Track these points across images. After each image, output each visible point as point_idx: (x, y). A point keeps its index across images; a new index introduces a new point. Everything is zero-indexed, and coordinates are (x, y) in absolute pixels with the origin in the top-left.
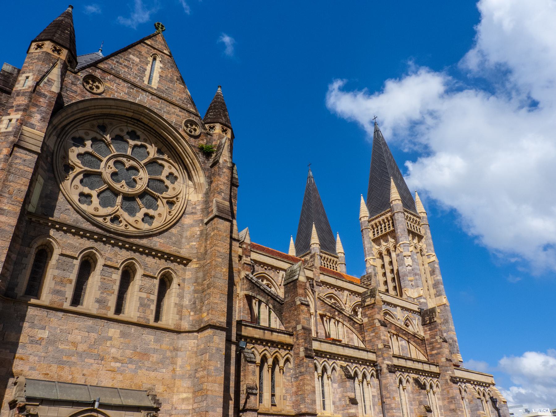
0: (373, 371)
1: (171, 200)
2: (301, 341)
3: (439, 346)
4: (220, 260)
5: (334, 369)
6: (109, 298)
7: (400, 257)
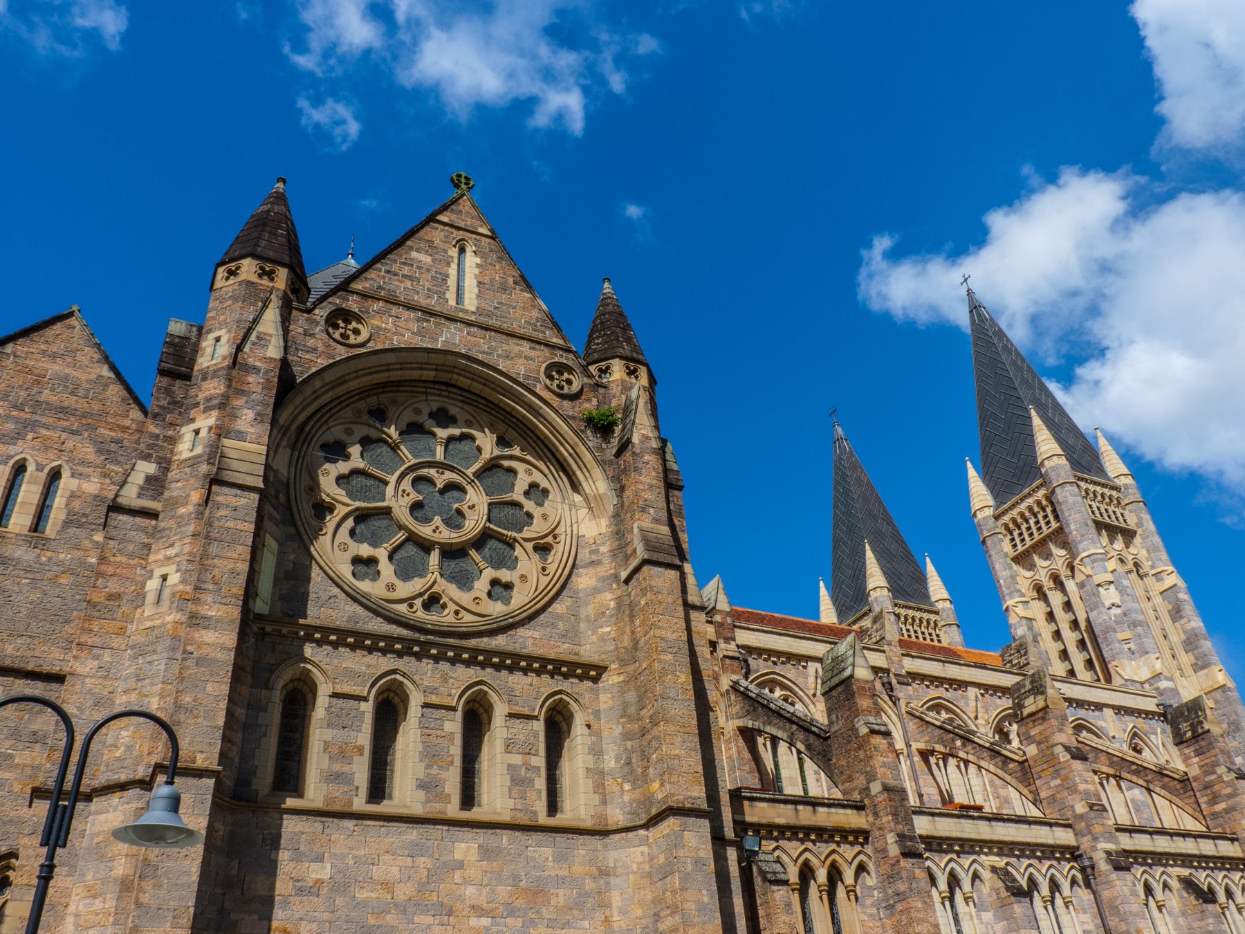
0: (1073, 872)
1: (542, 541)
2: (886, 819)
3: (1229, 790)
4: (670, 657)
5: (976, 876)
6: (444, 775)
7: (1088, 588)
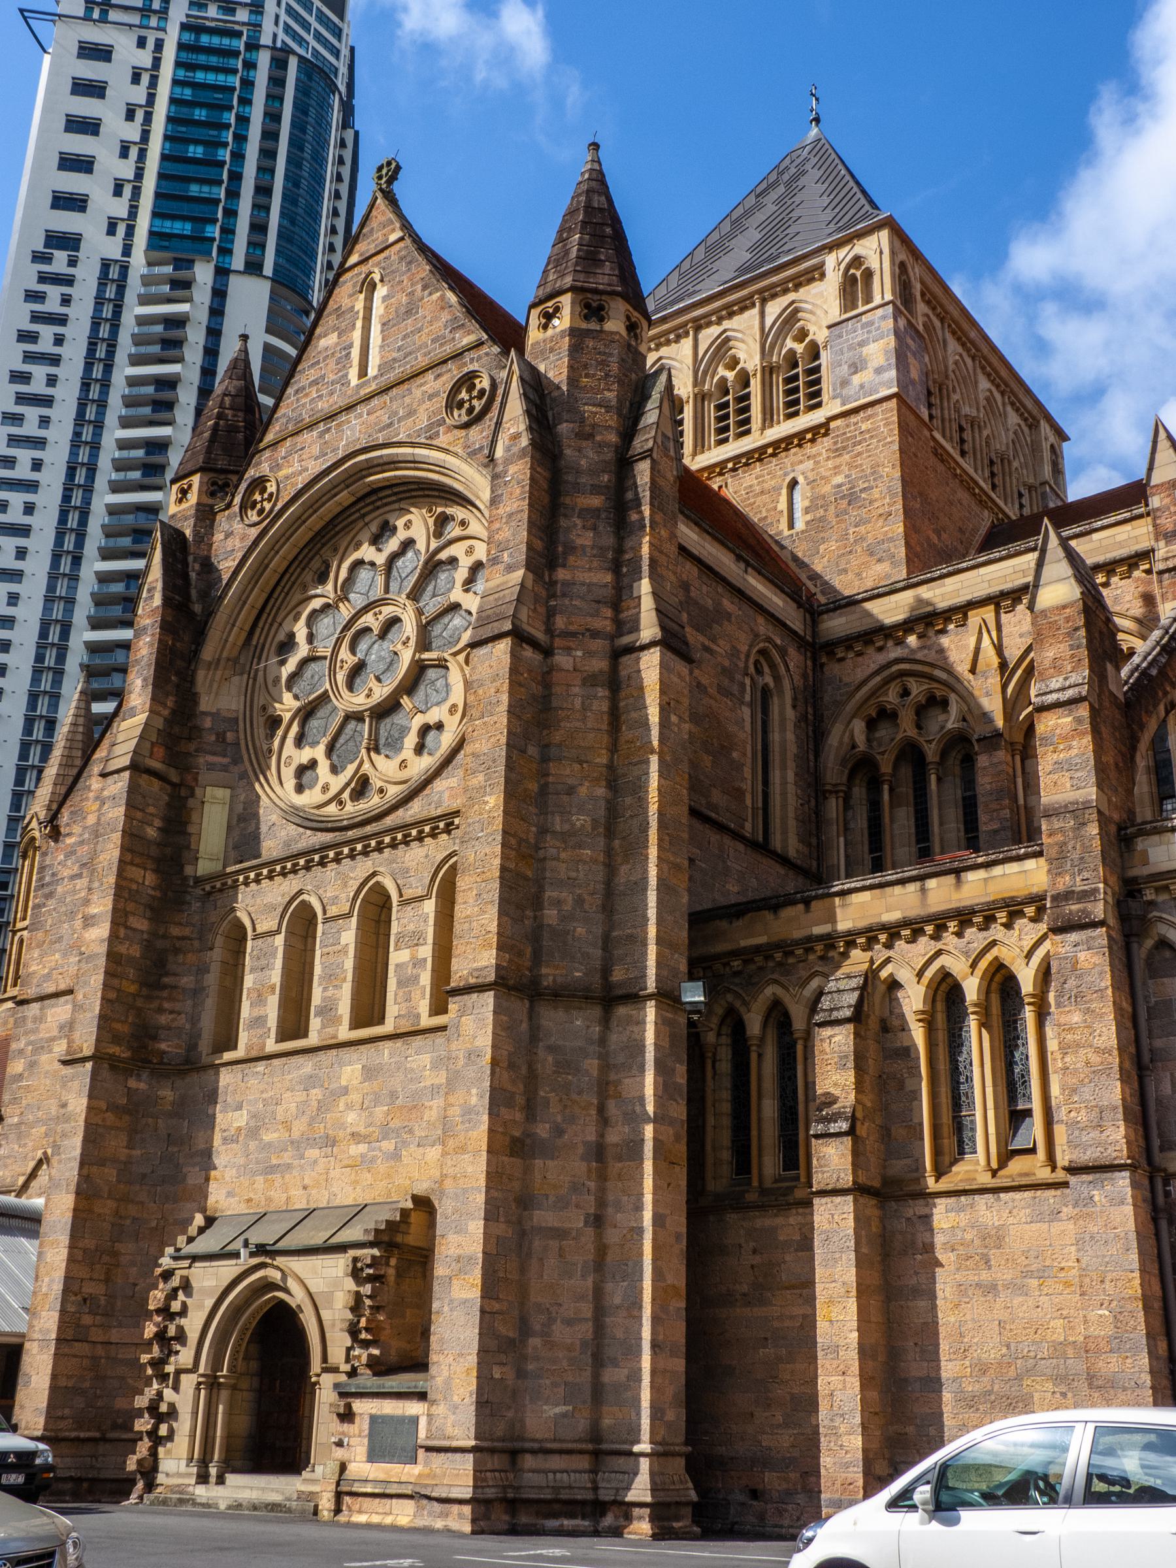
4: (481, 777)
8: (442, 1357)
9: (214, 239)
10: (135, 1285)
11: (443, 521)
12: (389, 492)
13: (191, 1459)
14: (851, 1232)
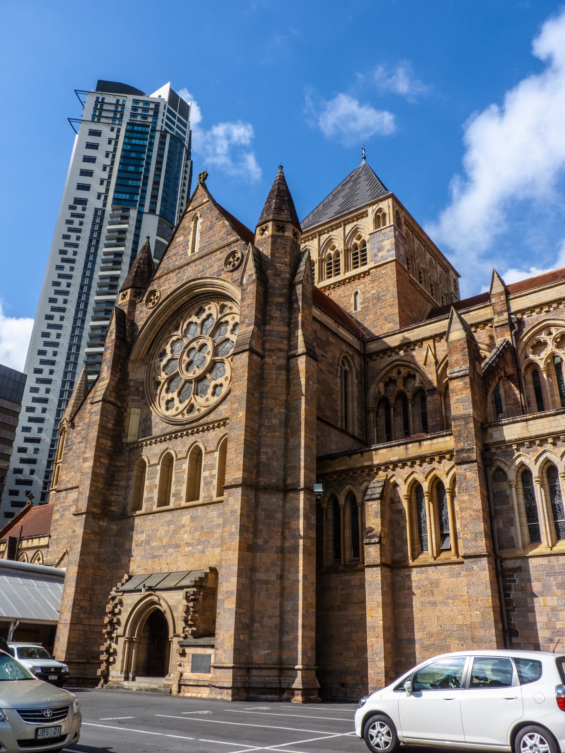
4: (237, 405)
8: (220, 631)
9: (137, 201)
10: (101, 602)
11: (223, 307)
12: (202, 296)
13: (122, 671)
14: (380, 581)
